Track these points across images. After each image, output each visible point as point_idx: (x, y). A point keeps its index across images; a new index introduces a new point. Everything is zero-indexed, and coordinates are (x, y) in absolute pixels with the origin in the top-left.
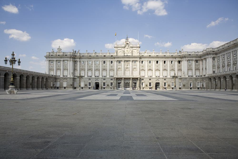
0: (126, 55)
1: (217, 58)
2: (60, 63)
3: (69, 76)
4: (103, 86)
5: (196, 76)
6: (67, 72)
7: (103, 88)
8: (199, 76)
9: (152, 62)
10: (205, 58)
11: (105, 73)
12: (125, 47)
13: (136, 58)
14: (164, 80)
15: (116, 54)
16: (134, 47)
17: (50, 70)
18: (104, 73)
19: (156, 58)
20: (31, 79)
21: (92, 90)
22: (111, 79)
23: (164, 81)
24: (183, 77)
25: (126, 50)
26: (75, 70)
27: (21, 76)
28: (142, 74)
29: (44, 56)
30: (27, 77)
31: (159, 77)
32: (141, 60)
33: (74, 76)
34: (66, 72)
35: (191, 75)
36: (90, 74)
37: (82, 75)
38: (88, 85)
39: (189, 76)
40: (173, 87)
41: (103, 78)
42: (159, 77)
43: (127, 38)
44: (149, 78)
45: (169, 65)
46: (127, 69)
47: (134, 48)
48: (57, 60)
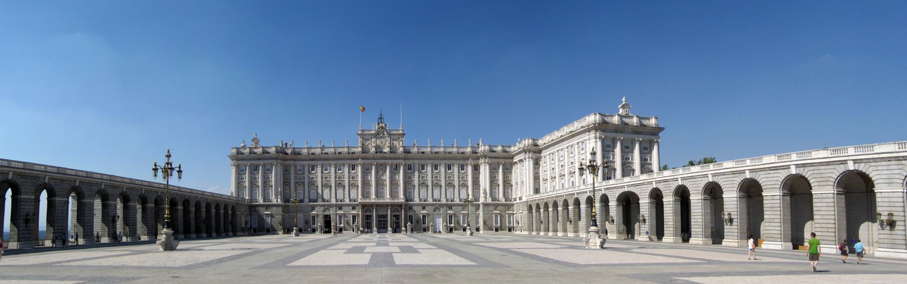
0: (379, 150)
10: (520, 159)
12: (378, 134)
15: (360, 149)
16: (393, 134)
20: (203, 210)
21: (318, 236)
22: (353, 207)
27: (186, 203)
30: (196, 206)
31: (439, 201)
32: (408, 162)
33: (285, 200)
38: (312, 223)
41: (338, 205)
42: (439, 201)
45: (456, 174)
47: (392, 137)
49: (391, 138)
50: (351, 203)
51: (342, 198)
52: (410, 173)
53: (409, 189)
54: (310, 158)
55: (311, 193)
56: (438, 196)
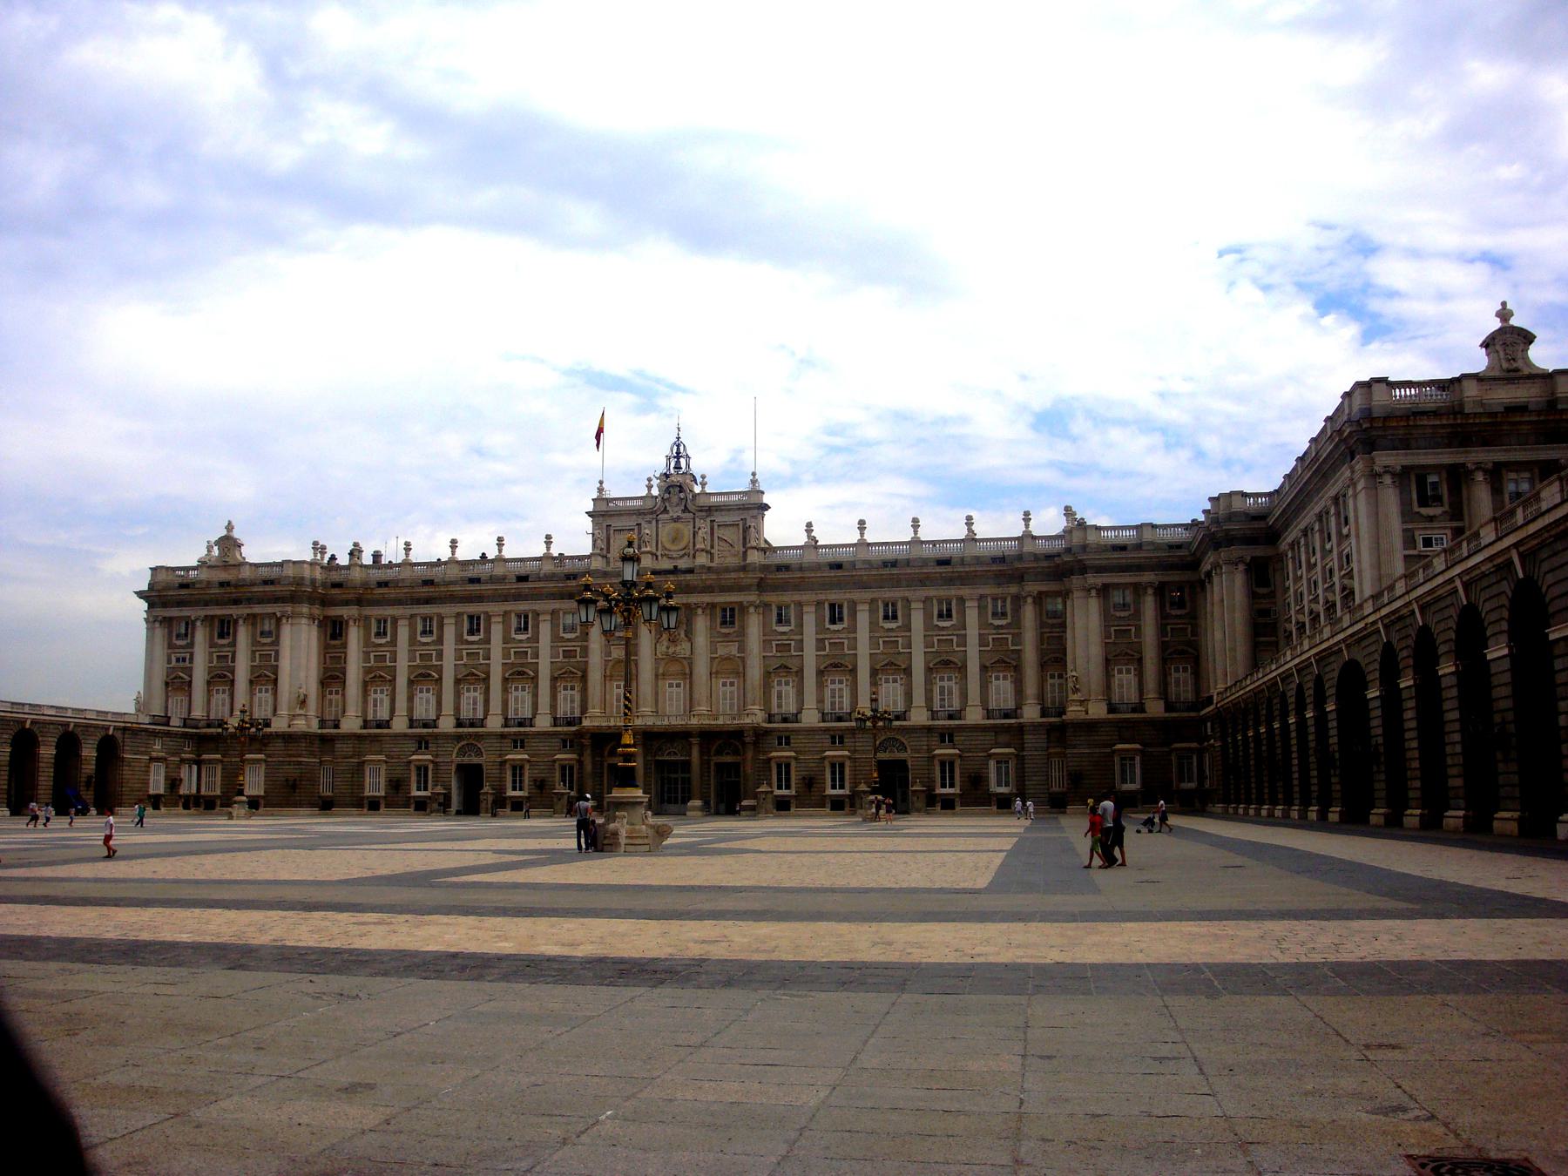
0: (666, 565)
1: (1282, 569)
2: (228, 634)
3: (279, 725)
4: (510, 793)
5: (1169, 707)
6: (269, 696)
7: (509, 806)
8: (1189, 709)
9: (853, 614)
11: (523, 702)
12: (665, 511)
13: (739, 588)
14: (943, 741)
16: (719, 508)
17: (177, 682)
18: (516, 699)
19: (881, 583)
23: (937, 752)
24: (1074, 712)
25: (666, 530)
26: (332, 677)
28: (780, 697)
29: (136, 592)
31: (897, 718)
32: (771, 598)
34: (263, 694)
35: (1134, 698)
36: (424, 707)
37: (375, 711)
38: (414, 786)
39: (1112, 709)
40: (1003, 790)
43: (675, 448)
44: (827, 730)
45: (972, 632)
46: (674, 668)
47: (720, 518)
48: (213, 617)
49: (712, 521)
50: (324, 731)
51: (527, 713)
52: (784, 633)
53: (780, 683)
54: (417, 596)
55: (417, 700)
56: (895, 703)
